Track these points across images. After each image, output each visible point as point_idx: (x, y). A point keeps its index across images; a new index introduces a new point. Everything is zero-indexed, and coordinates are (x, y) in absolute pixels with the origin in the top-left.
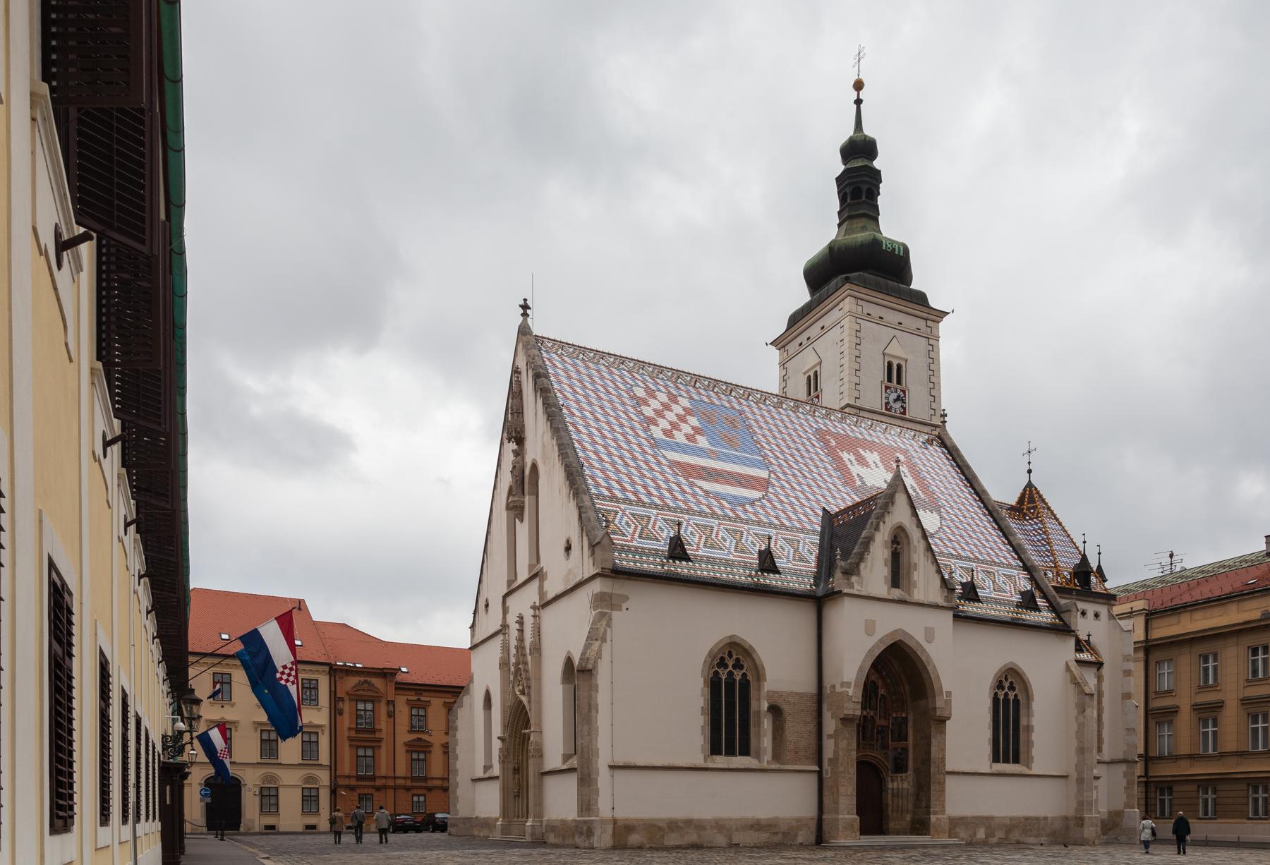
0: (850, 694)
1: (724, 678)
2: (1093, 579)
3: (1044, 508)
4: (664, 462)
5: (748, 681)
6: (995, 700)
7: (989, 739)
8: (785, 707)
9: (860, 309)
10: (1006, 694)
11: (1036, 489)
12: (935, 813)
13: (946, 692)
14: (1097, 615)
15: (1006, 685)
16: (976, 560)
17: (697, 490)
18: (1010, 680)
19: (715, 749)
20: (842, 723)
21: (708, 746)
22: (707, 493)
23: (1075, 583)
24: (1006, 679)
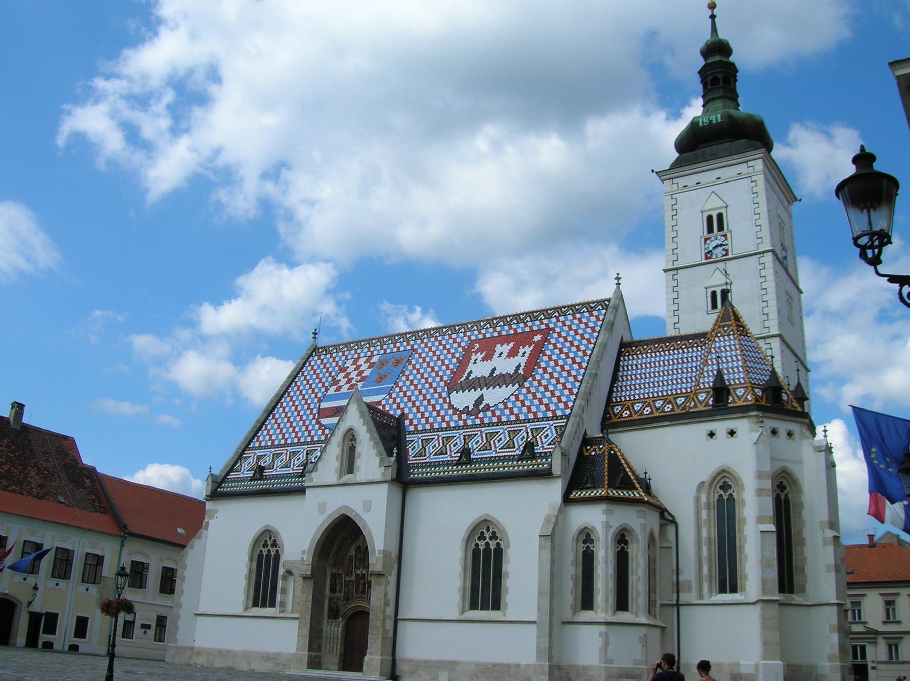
0: (305, 557)
1: (264, 554)
2: (740, 392)
3: (724, 326)
4: (315, 411)
5: (279, 555)
6: (476, 551)
7: (459, 588)
8: (295, 572)
9: (675, 186)
10: (487, 544)
11: (732, 307)
12: (371, 654)
13: (378, 550)
14: (732, 433)
15: (487, 535)
16: (518, 421)
17: (317, 427)
18: (491, 530)
19: (255, 604)
20: (304, 581)
21: (251, 601)
22: (321, 425)
23: (707, 405)
24: (488, 530)
